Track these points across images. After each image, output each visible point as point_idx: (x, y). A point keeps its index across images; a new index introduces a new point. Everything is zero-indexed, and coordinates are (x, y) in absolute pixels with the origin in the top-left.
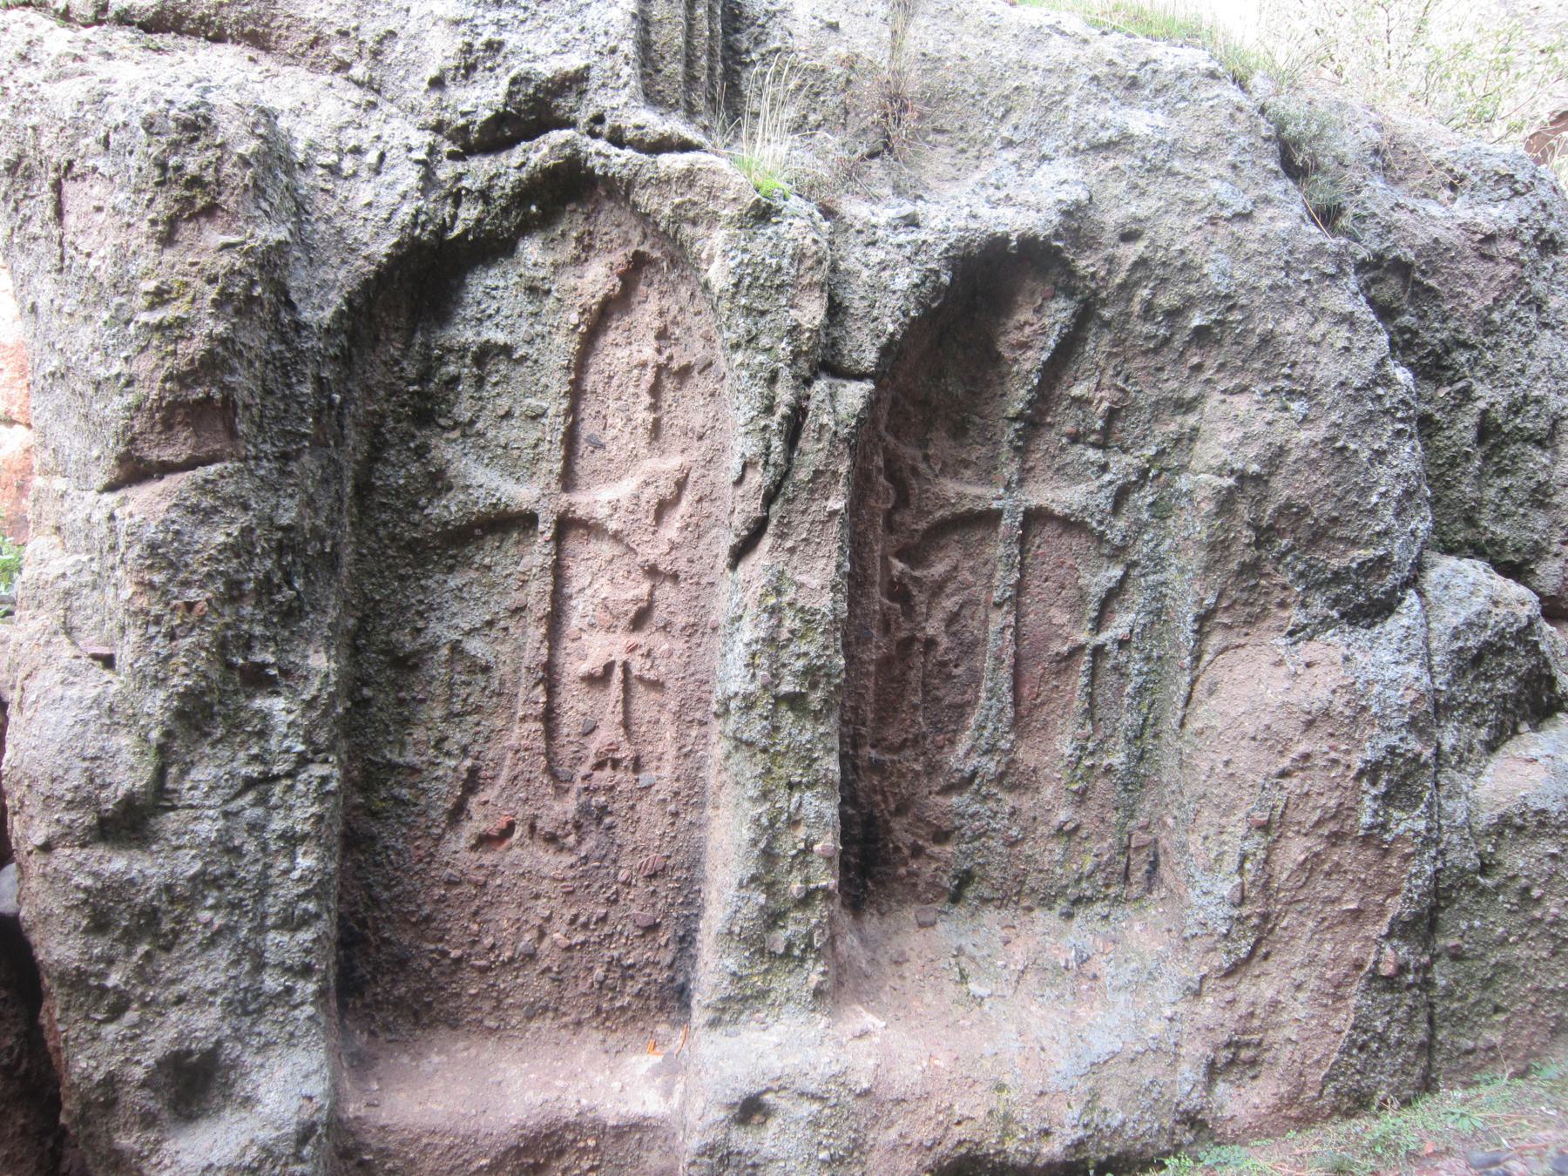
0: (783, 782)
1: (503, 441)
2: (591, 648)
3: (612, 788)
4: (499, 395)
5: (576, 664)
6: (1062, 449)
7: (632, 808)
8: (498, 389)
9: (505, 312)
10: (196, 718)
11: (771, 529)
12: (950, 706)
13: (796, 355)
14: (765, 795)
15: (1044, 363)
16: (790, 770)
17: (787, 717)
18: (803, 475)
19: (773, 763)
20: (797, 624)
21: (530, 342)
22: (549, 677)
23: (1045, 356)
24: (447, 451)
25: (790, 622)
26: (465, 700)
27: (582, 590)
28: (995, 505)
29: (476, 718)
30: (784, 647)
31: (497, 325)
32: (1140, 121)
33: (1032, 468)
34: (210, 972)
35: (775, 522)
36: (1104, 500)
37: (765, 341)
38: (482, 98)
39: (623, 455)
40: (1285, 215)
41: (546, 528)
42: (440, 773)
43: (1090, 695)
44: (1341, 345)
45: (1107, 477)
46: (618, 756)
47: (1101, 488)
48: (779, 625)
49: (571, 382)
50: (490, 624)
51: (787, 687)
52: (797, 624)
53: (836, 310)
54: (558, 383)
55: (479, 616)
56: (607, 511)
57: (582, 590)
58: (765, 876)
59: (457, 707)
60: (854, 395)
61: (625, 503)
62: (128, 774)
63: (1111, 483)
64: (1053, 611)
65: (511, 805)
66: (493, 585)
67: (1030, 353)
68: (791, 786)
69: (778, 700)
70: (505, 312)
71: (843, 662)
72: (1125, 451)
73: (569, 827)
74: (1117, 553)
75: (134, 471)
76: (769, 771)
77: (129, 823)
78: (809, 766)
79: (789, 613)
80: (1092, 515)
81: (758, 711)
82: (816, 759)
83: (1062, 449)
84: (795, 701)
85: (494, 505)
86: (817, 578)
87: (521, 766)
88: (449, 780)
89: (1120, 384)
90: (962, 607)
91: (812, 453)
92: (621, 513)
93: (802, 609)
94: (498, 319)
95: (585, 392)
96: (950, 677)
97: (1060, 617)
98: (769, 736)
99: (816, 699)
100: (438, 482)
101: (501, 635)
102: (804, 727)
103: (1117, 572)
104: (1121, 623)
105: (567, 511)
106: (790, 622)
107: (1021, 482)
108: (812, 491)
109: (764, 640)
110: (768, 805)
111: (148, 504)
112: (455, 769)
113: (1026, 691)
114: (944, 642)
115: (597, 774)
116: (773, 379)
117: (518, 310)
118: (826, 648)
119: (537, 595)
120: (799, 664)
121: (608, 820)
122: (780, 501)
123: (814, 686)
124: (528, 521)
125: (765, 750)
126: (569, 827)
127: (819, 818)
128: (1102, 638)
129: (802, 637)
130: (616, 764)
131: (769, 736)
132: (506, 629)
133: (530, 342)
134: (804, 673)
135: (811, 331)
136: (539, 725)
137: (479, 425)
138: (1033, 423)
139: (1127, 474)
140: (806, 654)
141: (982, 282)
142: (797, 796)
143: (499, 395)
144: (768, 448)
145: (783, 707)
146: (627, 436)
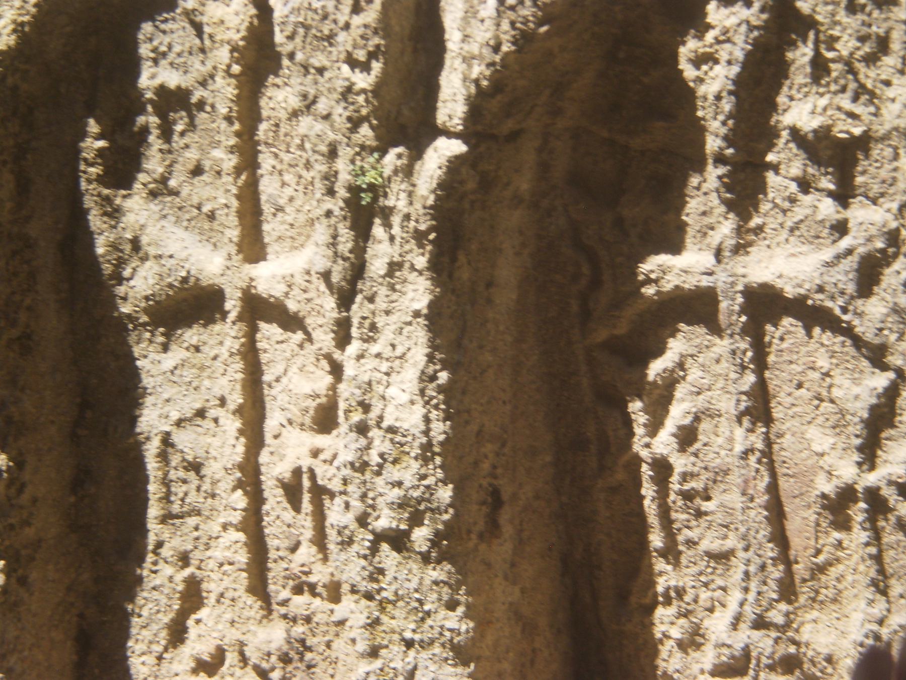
0: (396, 637)
1: (195, 200)
2: (290, 449)
3: (308, 620)
4: (187, 146)
5: (275, 467)
6: (792, 200)
7: (328, 645)
8: (186, 140)
9: (177, 49)
11: (354, 332)
12: (710, 555)
13: (355, 123)
14: (374, 652)
15: (735, 82)
16: (402, 623)
17: (388, 556)
18: (377, 266)
19: (383, 609)
20: (386, 447)
21: (203, 84)
22: (250, 478)
23: (736, 69)
25: (380, 444)
26: (182, 500)
27: (278, 380)
28: (705, 282)
29: (192, 521)
30: (379, 474)
31: (171, 64)
33: (759, 229)
35: (355, 321)
36: (844, 277)
37: (322, 106)
39: (302, 218)
41: (233, 305)
42: (158, 582)
43: (878, 559)
45: (846, 242)
46: (312, 579)
47: (838, 257)
48: (368, 447)
49: (238, 134)
50: (201, 413)
51: (385, 521)
52: (386, 447)
54: (228, 135)
55: (189, 405)
56: (283, 288)
57: (278, 380)
59: (176, 508)
61: (299, 280)
63: (849, 252)
64: (812, 432)
65: (220, 627)
66: (202, 368)
67: (717, 68)
68: (409, 644)
69: (379, 537)
70: (177, 49)
71: (450, 493)
72: (874, 201)
73: (274, 659)
74: (877, 356)
76: (377, 622)
78: (423, 620)
79: (374, 433)
80: (832, 298)
81: (355, 547)
82: (428, 614)
83: (792, 200)
84: (398, 541)
85: (185, 280)
87: (227, 582)
88: (166, 591)
89: (847, 104)
90: (697, 419)
92: (296, 291)
93: (392, 430)
94: (171, 56)
95: (258, 143)
96: (699, 514)
97: (820, 439)
98: (372, 578)
99: (421, 536)
101: (212, 425)
102: (410, 571)
103: (882, 380)
105: (249, 287)
106: (380, 444)
107: (740, 249)
108: (392, 288)
109: (352, 464)
110: (378, 663)
112: (171, 579)
113: (796, 542)
114: (680, 463)
115: (298, 600)
116: (332, 153)
117: (187, 45)
118: (423, 477)
119: (228, 382)
120: (395, 494)
121: (308, 656)
122: (359, 298)
123: (416, 520)
125: (369, 596)
126: (274, 659)
128: (871, 479)
129: (395, 462)
130: (312, 589)
131: (372, 578)
132: (216, 420)
133: (203, 84)
134: (401, 506)
135: (364, 91)
136: (241, 536)
137: (172, 183)
139: (869, 240)
140: (399, 484)
142: (412, 653)
143: (187, 146)
144: (335, 237)
145: (385, 547)
146: (301, 194)
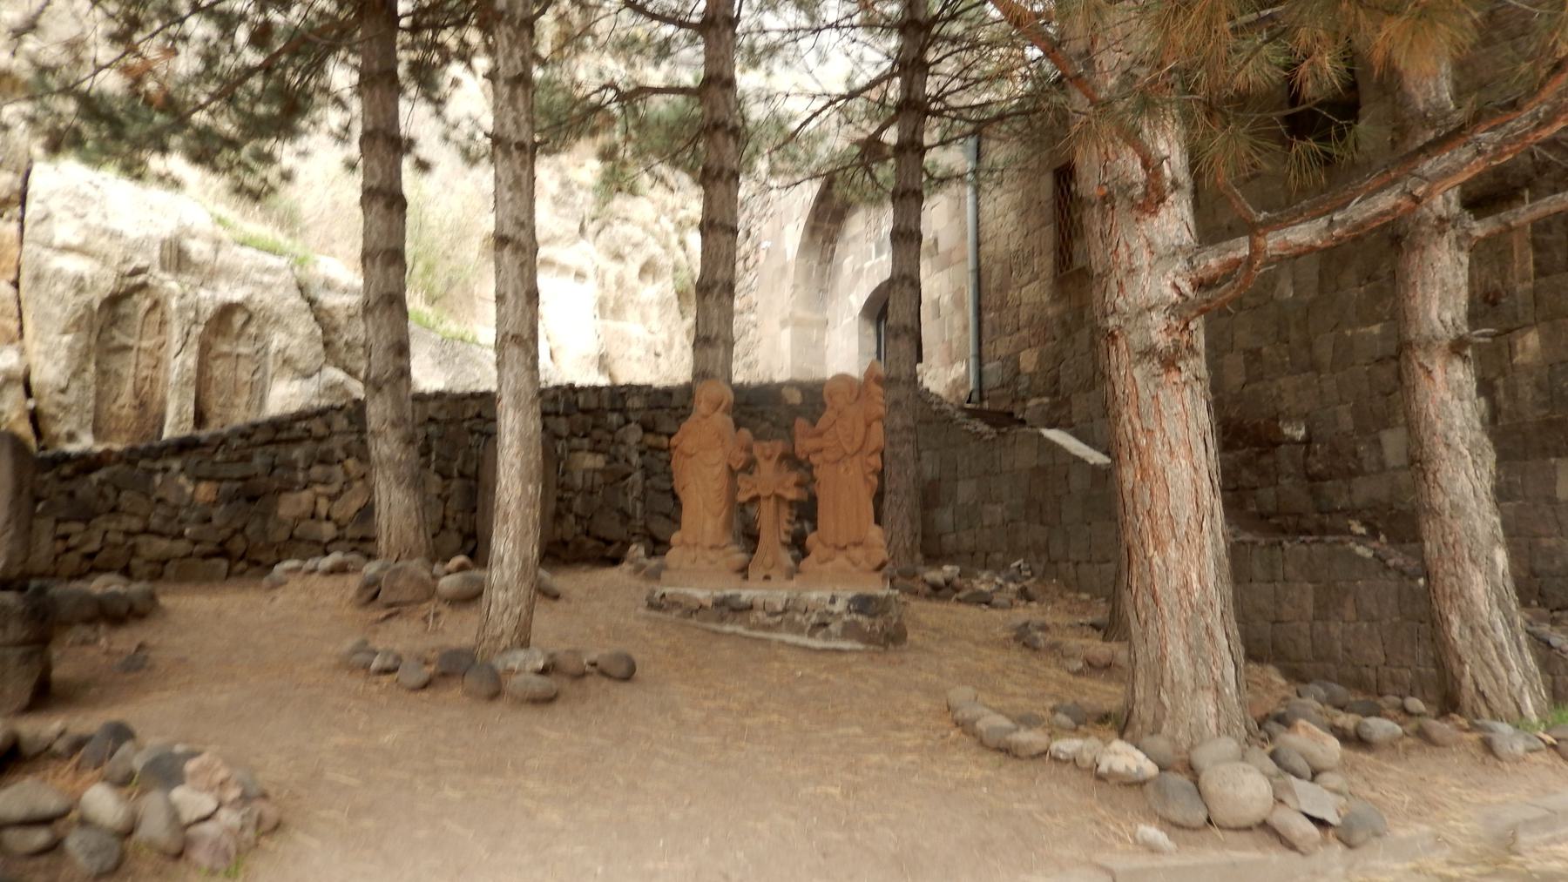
10: (76, 375)
24: (115, 332)
32: (267, 278)
34: (75, 418)
38: (129, 268)
40: (295, 299)
44: (304, 325)
53: (197, 313)
58: (179, 413)
60: (200, 329)
62: (63, 384)
75: (65, 332)
77: (63, 391)
86: (191, 362)
91: (191, 340)
100: (113, 338)
104: (257, 377)
111: (67, 339)
124: (131, 348)
127: (190, 408)
138: (239, 336)
141: (227, 311)
